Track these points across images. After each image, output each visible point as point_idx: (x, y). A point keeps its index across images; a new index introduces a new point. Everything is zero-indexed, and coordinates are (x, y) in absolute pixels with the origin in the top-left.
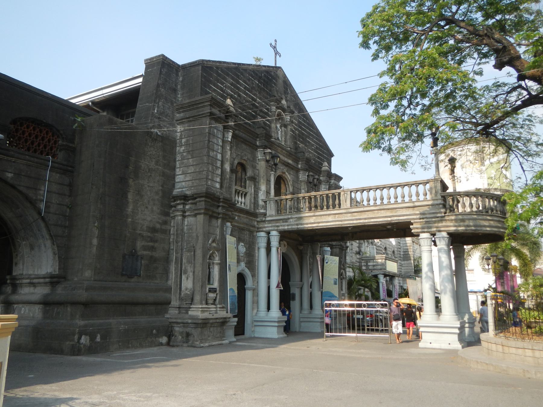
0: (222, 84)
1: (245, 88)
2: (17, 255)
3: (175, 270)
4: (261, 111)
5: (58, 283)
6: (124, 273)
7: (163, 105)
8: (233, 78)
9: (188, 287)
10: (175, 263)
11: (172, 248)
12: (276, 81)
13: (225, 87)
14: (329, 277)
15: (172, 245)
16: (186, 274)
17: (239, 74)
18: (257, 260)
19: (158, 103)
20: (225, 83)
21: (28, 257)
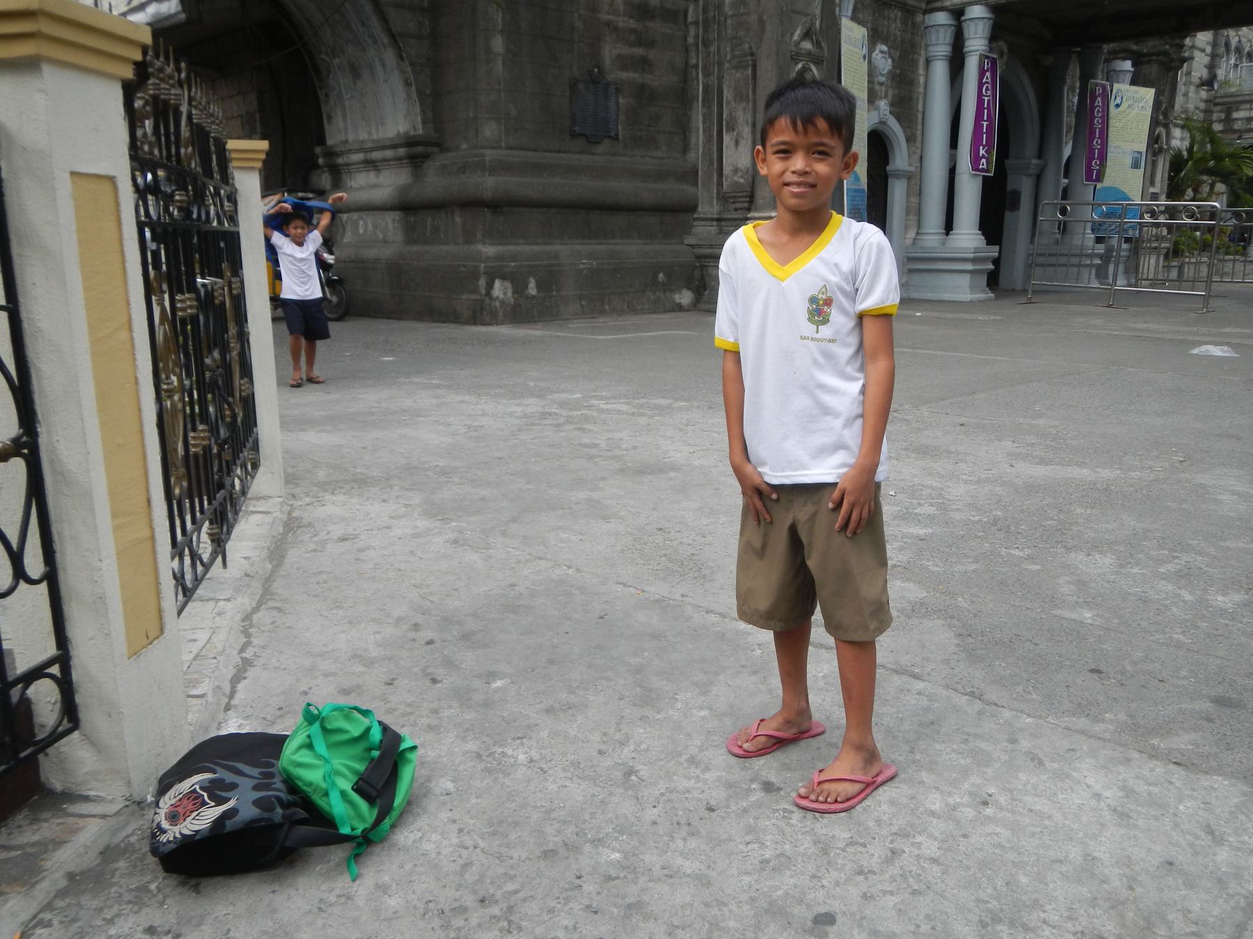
2: (327, 95)
3: (704, 122)
5: (426, 156)
6: (577, 129)
9: (740, 166)
10: (703, 101)
11: (694, 61)
14: (1118, 147)
15: (692, 54)
16: (733, 130)
18: (921, 97)
21: (352, 97)
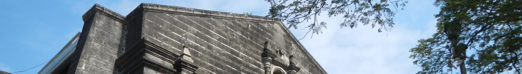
0: (181, 33)
1: (220, 39)
4: (247, 67)
7: (95, 61)
8: (198, 28)
12: (272, 34)
13: (186, 36)
17: (210, 23)
19: (88, 59)
20: (185, 33)
